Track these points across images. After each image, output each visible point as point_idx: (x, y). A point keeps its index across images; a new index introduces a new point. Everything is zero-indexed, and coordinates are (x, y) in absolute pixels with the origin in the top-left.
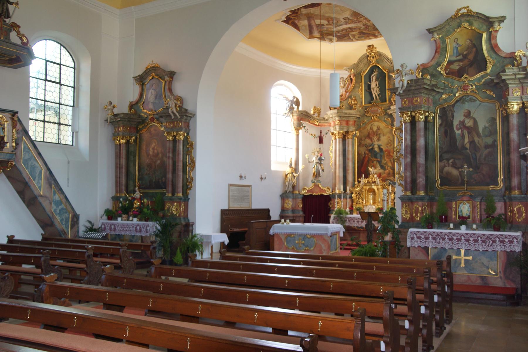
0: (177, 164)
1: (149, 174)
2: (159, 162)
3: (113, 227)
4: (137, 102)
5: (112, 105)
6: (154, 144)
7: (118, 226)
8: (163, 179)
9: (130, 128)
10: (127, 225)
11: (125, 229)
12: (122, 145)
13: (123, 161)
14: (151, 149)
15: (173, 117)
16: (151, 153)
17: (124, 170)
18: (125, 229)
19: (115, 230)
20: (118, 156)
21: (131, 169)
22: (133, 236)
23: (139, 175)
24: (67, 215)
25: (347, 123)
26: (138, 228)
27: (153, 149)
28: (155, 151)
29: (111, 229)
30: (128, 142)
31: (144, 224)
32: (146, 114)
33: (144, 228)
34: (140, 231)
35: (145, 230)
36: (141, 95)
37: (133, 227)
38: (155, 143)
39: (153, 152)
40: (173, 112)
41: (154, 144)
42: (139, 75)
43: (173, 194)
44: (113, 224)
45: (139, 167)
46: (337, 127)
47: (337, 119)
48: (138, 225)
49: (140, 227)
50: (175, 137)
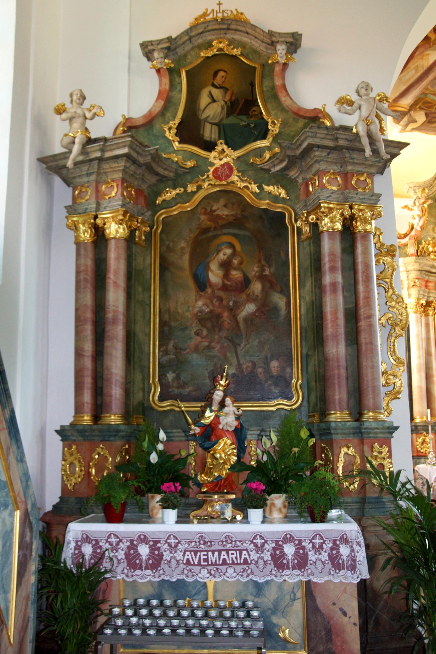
0: (362, 311)
1: (209, 348)
2: (250, 308)
3: (144, 550)
4: (150, 122)
5: (87, 104)
6: (229, 251)
7: (173, 548)
8: (274, 364)
9: (139, 192)
10: (228, 538)
11: (213, 558)
12: (112, 245)
13: (116, 298)
14: (214, 266)
15: (368, 152)
16: (215, 276)
17: (117, 332)
18: (213, 558)
19: (156, 561)
20: (96, 278)
21: (139, 329)
22: (259, 588)
23: (164, 352)
24: (5, 514)
25: (426, 286)
26: (289, 550)
27: (226, 266)
28: (236, 274)
29: (133, 561)
30: (130, 240)
31: (318, 534)
32: (193, 155)
33: (319, 549)
34: (302, 562)
35: (325, 556)
36: (167, 100)
37: (259, 549)
38: (232, 246)
39: (226, 276)
40: (370, 136)
41: (229, 251)
42: (169, 39)
43: (358, 416)
44: (143, 539)
45: (162, 324)
46: (414, 292)
47: (413, 275)
48: (288, 538)
49: (299, 546)
50: (349, 224)
